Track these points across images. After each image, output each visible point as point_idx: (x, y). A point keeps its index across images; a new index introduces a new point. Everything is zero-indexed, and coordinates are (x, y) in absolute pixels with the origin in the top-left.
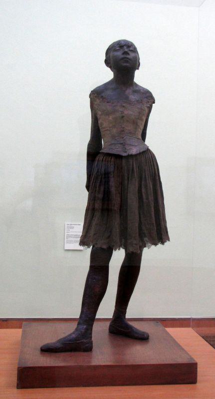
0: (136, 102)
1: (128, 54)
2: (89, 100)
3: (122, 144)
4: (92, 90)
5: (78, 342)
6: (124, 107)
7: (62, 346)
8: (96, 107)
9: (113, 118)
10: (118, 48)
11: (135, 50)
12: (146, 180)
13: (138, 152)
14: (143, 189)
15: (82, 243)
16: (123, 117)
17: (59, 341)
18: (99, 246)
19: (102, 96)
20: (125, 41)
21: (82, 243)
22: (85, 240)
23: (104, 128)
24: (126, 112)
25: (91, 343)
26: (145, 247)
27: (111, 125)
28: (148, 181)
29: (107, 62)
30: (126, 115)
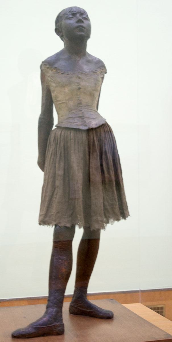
0: (91, 73)
1: (83, 22)
3: (80, 117)
4: (43, 60)
5: (51, 325)
6: (79, 78)
7: (34, 331)
8: (49, 79)
10: (71, 16)
11: (87, 19)
13: (98, 126)
15: (43, 221)
16: (79, 89)
17: (32, 326)
18: (62, 225)
19: (56, 67)
20: (76, 8)
21: (43, 221)
22: (46, 219)
23: (59, 101)
25: (63, 325)
26: (108, 223)
27: (67, 98)
29: (58, 31)
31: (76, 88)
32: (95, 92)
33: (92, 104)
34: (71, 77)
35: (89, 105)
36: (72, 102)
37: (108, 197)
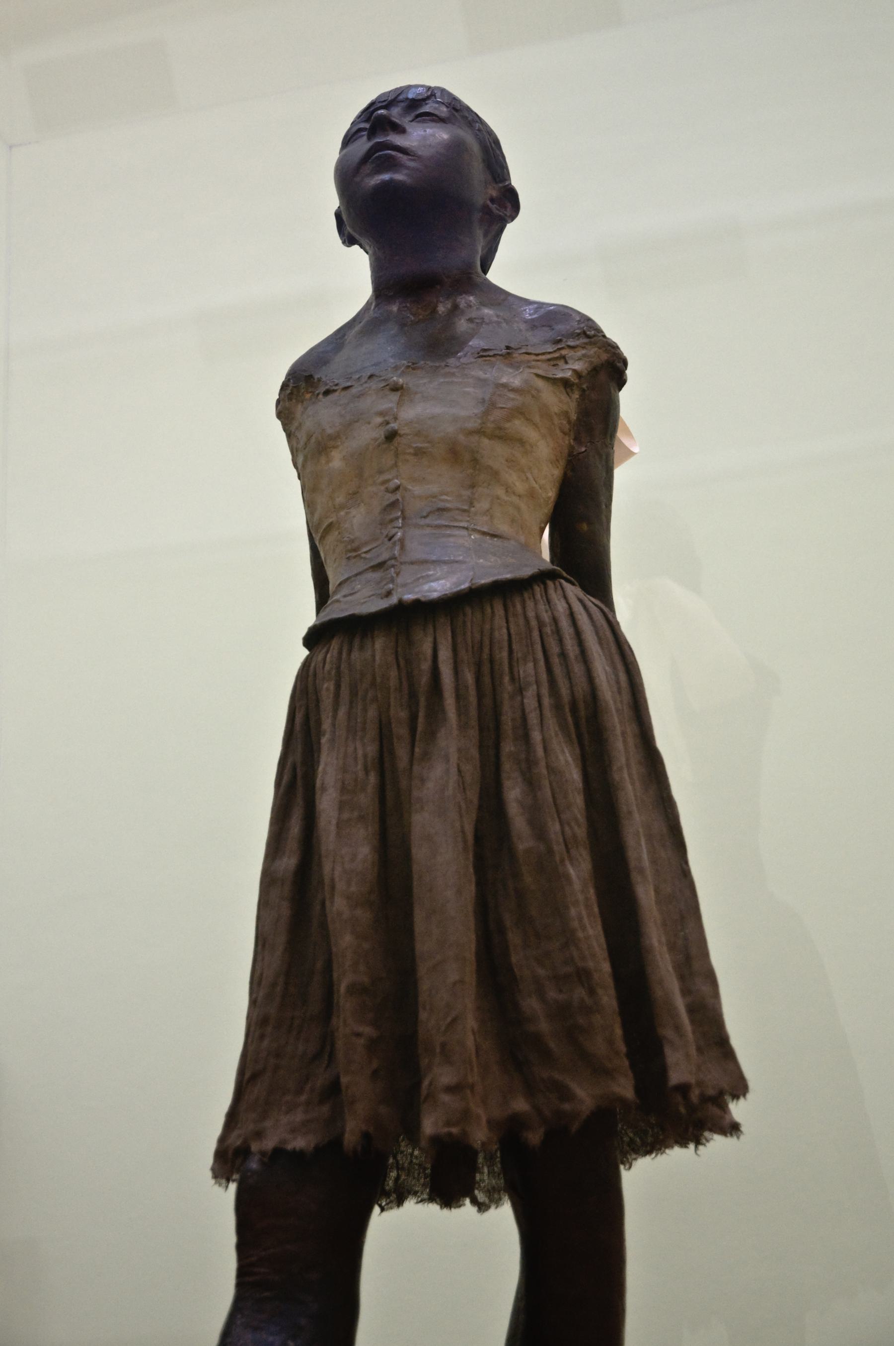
2: (278, 424)
6: (396, 388)
9: (344, 458)
12: (525, 737)
14: (507, 783)
16: (391, 436)
24: (411, 412)
28: (536, 736)
30: (410, 422)
31: (376, 440)
32: (486, 441)
33: (472, 505)
34: (360, 396)
35: (448, 505)
36: (362, 509)
37: (541, 972)
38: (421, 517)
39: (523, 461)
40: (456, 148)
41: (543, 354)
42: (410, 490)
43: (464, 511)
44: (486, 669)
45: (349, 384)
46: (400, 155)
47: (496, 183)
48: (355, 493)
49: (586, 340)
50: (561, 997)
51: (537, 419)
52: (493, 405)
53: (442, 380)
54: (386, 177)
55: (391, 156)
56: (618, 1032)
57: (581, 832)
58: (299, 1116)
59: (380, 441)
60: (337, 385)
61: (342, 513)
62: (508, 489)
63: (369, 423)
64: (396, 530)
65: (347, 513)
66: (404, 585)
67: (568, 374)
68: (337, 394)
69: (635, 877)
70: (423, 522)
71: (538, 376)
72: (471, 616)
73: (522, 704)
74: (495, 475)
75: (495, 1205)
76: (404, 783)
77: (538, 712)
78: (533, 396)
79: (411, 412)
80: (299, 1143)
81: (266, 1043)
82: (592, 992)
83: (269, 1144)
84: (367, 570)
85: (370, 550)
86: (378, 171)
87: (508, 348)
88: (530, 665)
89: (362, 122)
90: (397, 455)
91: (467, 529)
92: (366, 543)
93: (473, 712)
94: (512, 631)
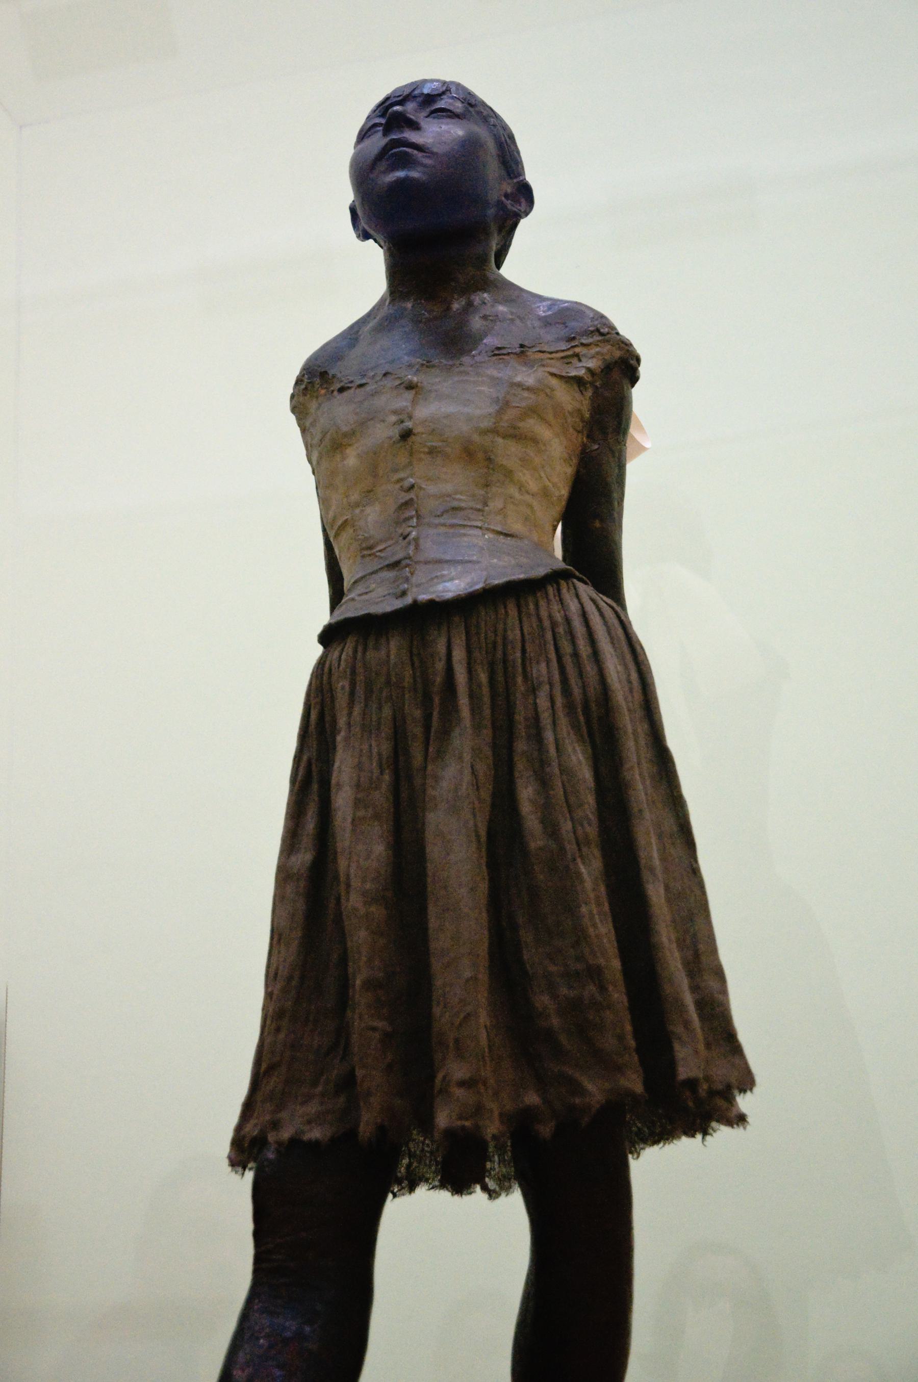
2: (292, 418)
6: (410, 387)
9: (359, 456)
12: (537, 737)
14: (520, 783)
16: (406, 435)
24: (424, 412)
28: (549, 736)
30: (424, 422)
31: (390, 438)
32: (500, 440)
33: (485, 504)
35: (463, 505)
36: (377, 507)
37: (553, 968)
38: (436, 516)
39: (537, 460)
40: (470, 146)
41: (557, 352)
42: (424, 489)
43: (479, 510)
44: (499, 668)
45: (364, 381)
46: (415, 152)
47: (511, 178)
48: (369, 491)
49: (600, 338)
50: (572, 994)
51: (550, 417)
52: (507, 403)
53: (456, 379)
54: (401, 174)
55: (406, 153)
56: (629, 1028)
57: (592, 831)
58: (313, 1108)
59: (394, 439)
60: (352, 382)
61: (357, 511)
62: (521, 487)
63: (383, 421)
64: (411, 529)
65: (362, 511)
66: (418, 585)
67: (582, 372)
68: (352, 391)
69: (646, 875)
70: (437, 521)
71: (553, 375)
72: (485, 616)
73: (536, 704)
74: (509, 474)
75: (506, 1193)
76: (418, 781)
77: (551, 711)
78: (547, 395)
79: (424, 412)
80: (315, 1134)
81: (282, 1036)
82: (602, 988)
83: (286, 1134)
84: (381, 569)
85: (385, 549)
86: (393, 168)
87: (522, 346)
88: (543, 665)
89: (377, 117)
90: (411, 454)
91: (481, 528)
92: (381, 541)
93: (487, 712)
94: (525, 631)
